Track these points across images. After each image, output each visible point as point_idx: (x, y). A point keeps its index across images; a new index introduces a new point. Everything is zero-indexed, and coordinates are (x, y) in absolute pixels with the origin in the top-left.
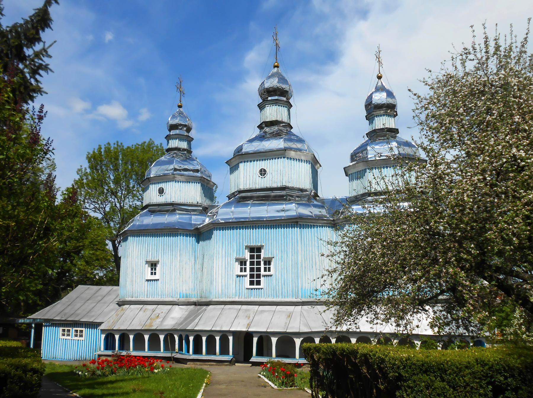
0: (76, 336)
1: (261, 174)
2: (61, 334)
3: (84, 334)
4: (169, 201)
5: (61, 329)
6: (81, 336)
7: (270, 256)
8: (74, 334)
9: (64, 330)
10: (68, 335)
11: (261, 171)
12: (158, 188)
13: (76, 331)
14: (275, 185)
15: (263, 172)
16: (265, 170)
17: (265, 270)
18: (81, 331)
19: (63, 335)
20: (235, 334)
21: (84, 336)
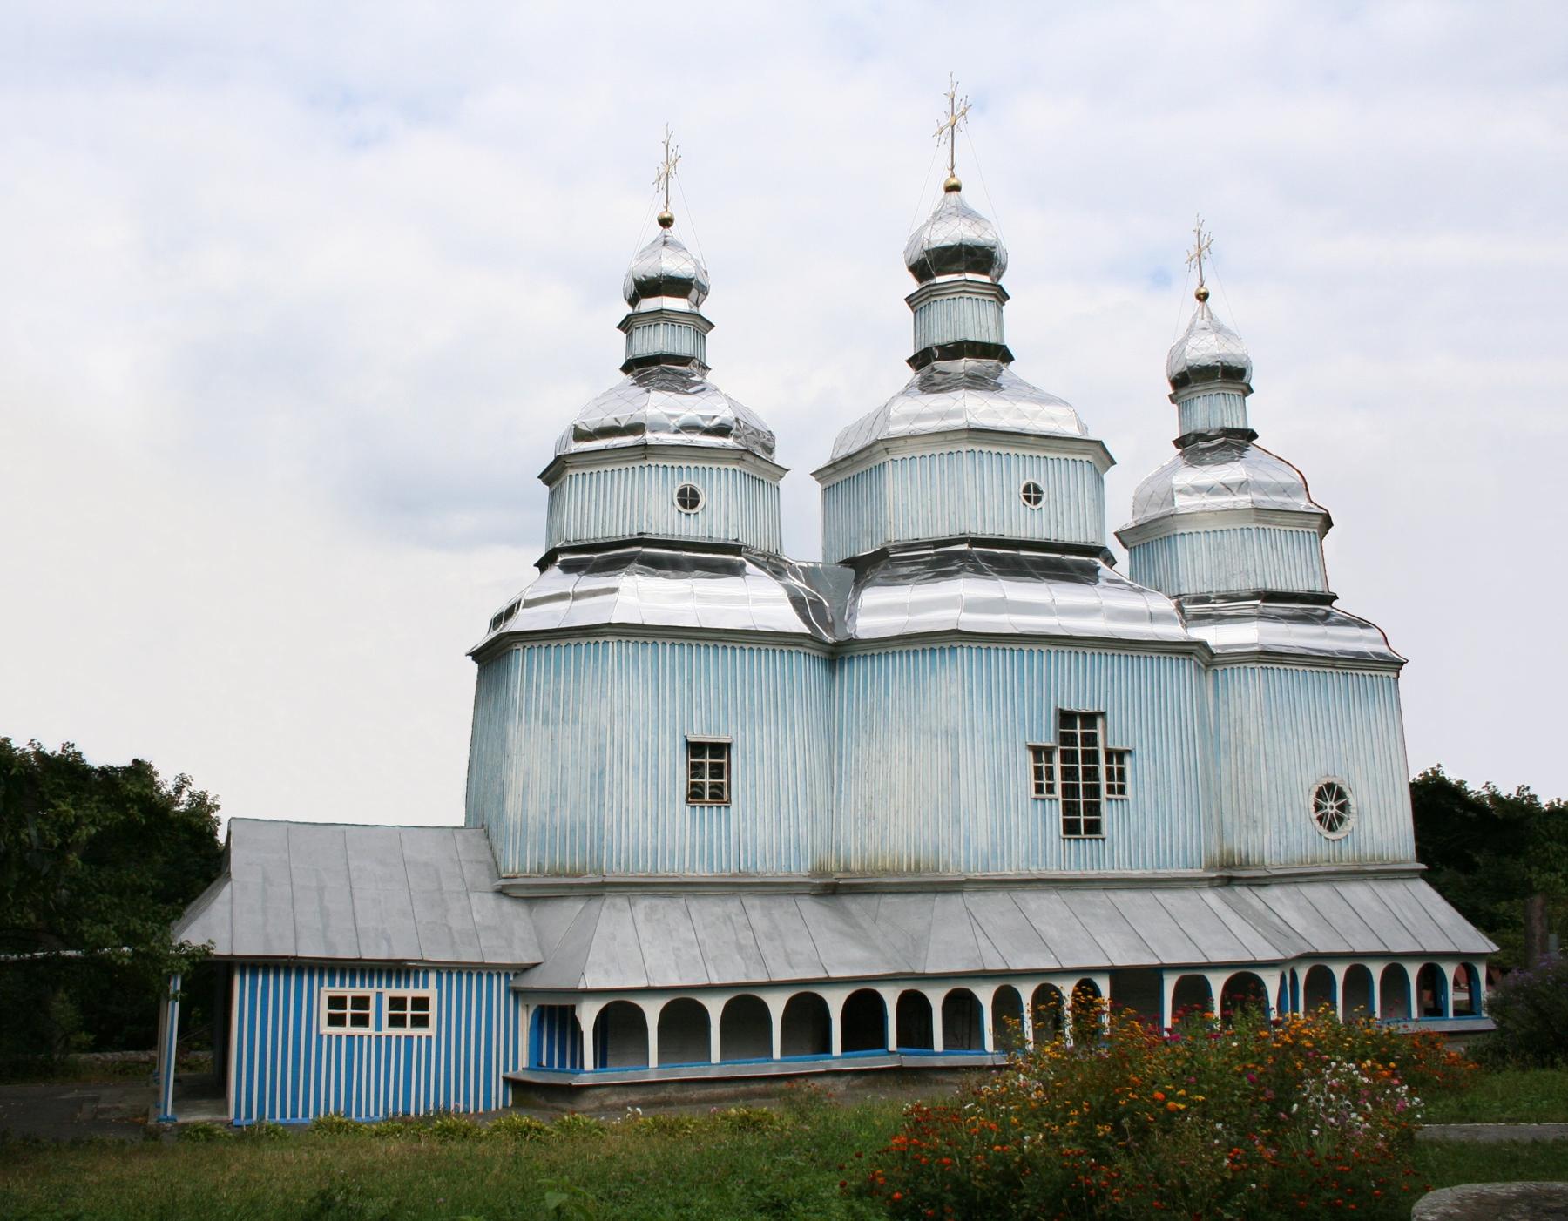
0: (397, 1021)
1: (1028, 498)
2: (324, 1019)
3: (432, 1012)
4: (719, 535)
5: (327, 991)
6: (421, 1021)
7: (1125, 747)
8: (372, 1012)
9: (336, 1002)
10: (361, 1021)
11: (1027, 489)
12: (678, 488)
13: (397, 1003)
14: (1068, 537)
15: (1032, 494)
16: (1037, 489)
17: (1110, 789)
18: (421, 1003)
19: (336, 1020)
20: (1115, 973)
21: (433, 1020)
